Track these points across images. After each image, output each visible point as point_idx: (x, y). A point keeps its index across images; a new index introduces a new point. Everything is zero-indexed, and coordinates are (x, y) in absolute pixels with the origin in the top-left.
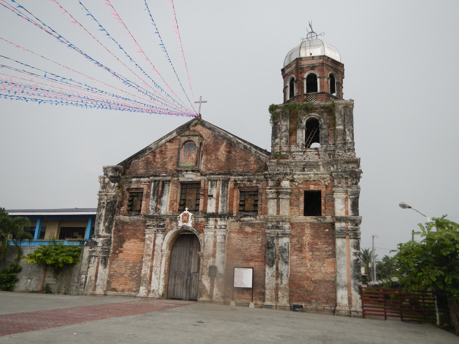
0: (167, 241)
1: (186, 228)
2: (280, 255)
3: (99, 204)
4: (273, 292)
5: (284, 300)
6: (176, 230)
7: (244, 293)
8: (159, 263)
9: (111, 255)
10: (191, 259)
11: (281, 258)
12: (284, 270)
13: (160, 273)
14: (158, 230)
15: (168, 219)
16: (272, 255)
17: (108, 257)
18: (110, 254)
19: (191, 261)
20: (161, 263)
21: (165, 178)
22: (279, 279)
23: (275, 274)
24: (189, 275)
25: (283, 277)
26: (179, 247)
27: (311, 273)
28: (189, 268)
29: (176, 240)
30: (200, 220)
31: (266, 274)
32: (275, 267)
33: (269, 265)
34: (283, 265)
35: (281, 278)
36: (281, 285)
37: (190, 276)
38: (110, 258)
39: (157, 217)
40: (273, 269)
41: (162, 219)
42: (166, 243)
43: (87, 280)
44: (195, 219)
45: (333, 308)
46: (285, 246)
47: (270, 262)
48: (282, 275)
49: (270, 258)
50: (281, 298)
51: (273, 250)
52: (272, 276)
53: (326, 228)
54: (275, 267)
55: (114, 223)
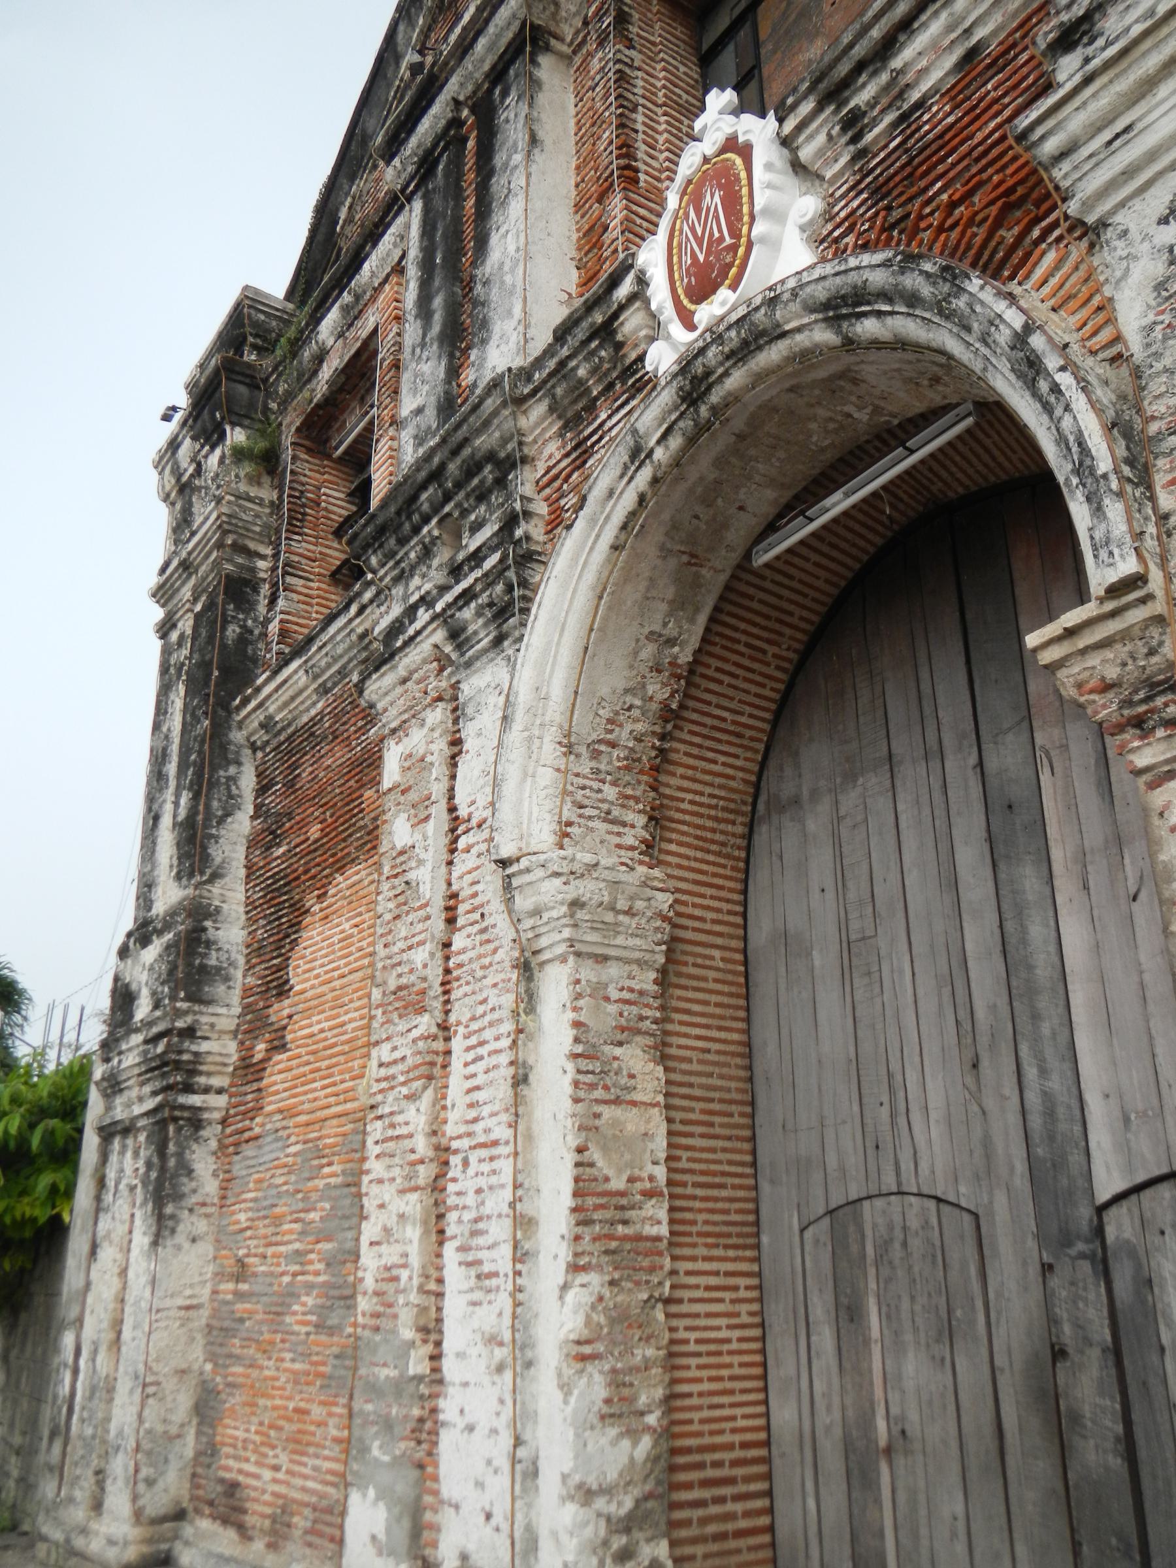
0: (555, 710)
1: (741, 353)
3: (164, 669)
6: (628, 500)
8: (502, 1091)
9: (221, 1101)
10: (1037, 931)
13: (521, 1255)
14: (456, 634)
15: (538, 409)
17: (195, 1119)
18: (216, 1082)
19: (1043, 972)
20: (521, 1080)
21: (482, 43)
24: (1066, 1239)
26: (825, 806)
28: (1050, 1113)
29: (775, 723)
30: (934, 45)
37: (1104, 1270)
38: (224, 1122)
39: (436, 475)
41: (488, 473)
42: (550, 751)
43: (79, 1385)
44: (854, 124)
55: (248, 781)
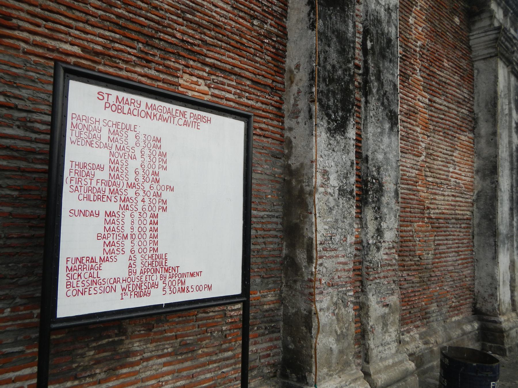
2: (372, 69)
4: (346, 306)
5: (388, 338)
7: (129, 353)
11: (374, 86)
12: (386, 159)
16: (344, 50)
22: (369, 214)
23: (353, 179)
25: (385, 199)
27: (427, 185)
31: (319, 179)
32: (352, 133)
33: (328, 115)
34: (382, 133)
35: (378, 209)
36: (378, 249)
40: (345, 150)
45: (476, 325)
46: (388, 22)
47: (334, 94)
48: (380, 190)
49: (333, 67)
50: (379, 329)
51: (345, 22)
52: (342, 192)
53: (454, 12)
54: (352, 133)
